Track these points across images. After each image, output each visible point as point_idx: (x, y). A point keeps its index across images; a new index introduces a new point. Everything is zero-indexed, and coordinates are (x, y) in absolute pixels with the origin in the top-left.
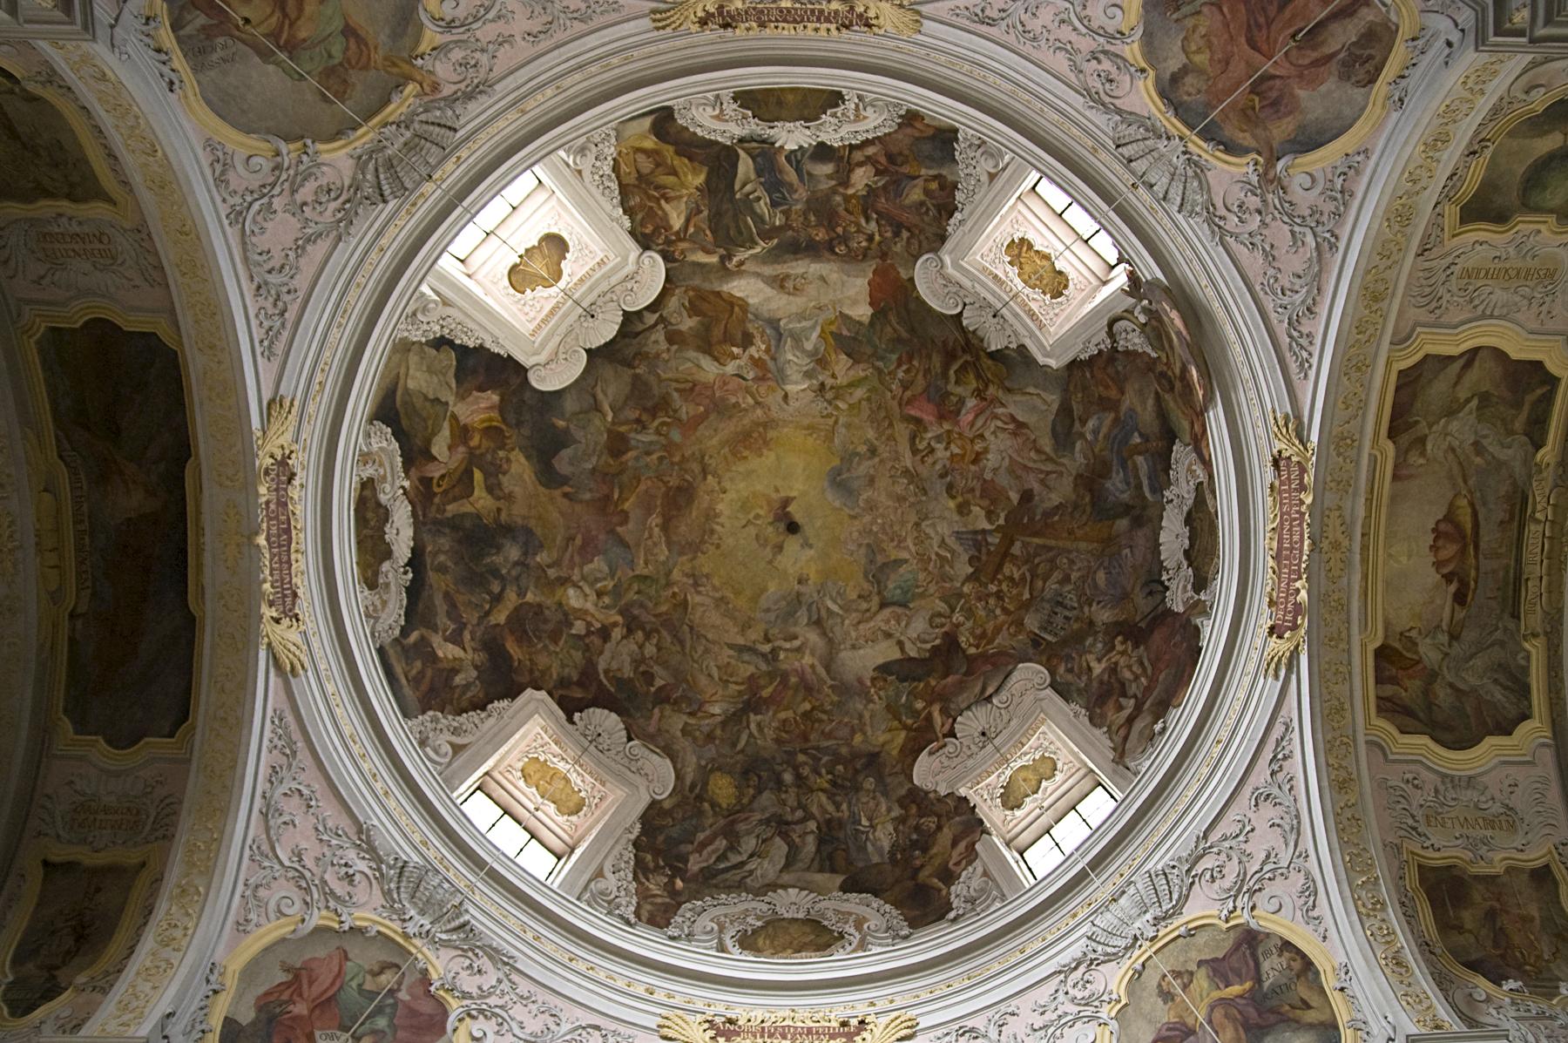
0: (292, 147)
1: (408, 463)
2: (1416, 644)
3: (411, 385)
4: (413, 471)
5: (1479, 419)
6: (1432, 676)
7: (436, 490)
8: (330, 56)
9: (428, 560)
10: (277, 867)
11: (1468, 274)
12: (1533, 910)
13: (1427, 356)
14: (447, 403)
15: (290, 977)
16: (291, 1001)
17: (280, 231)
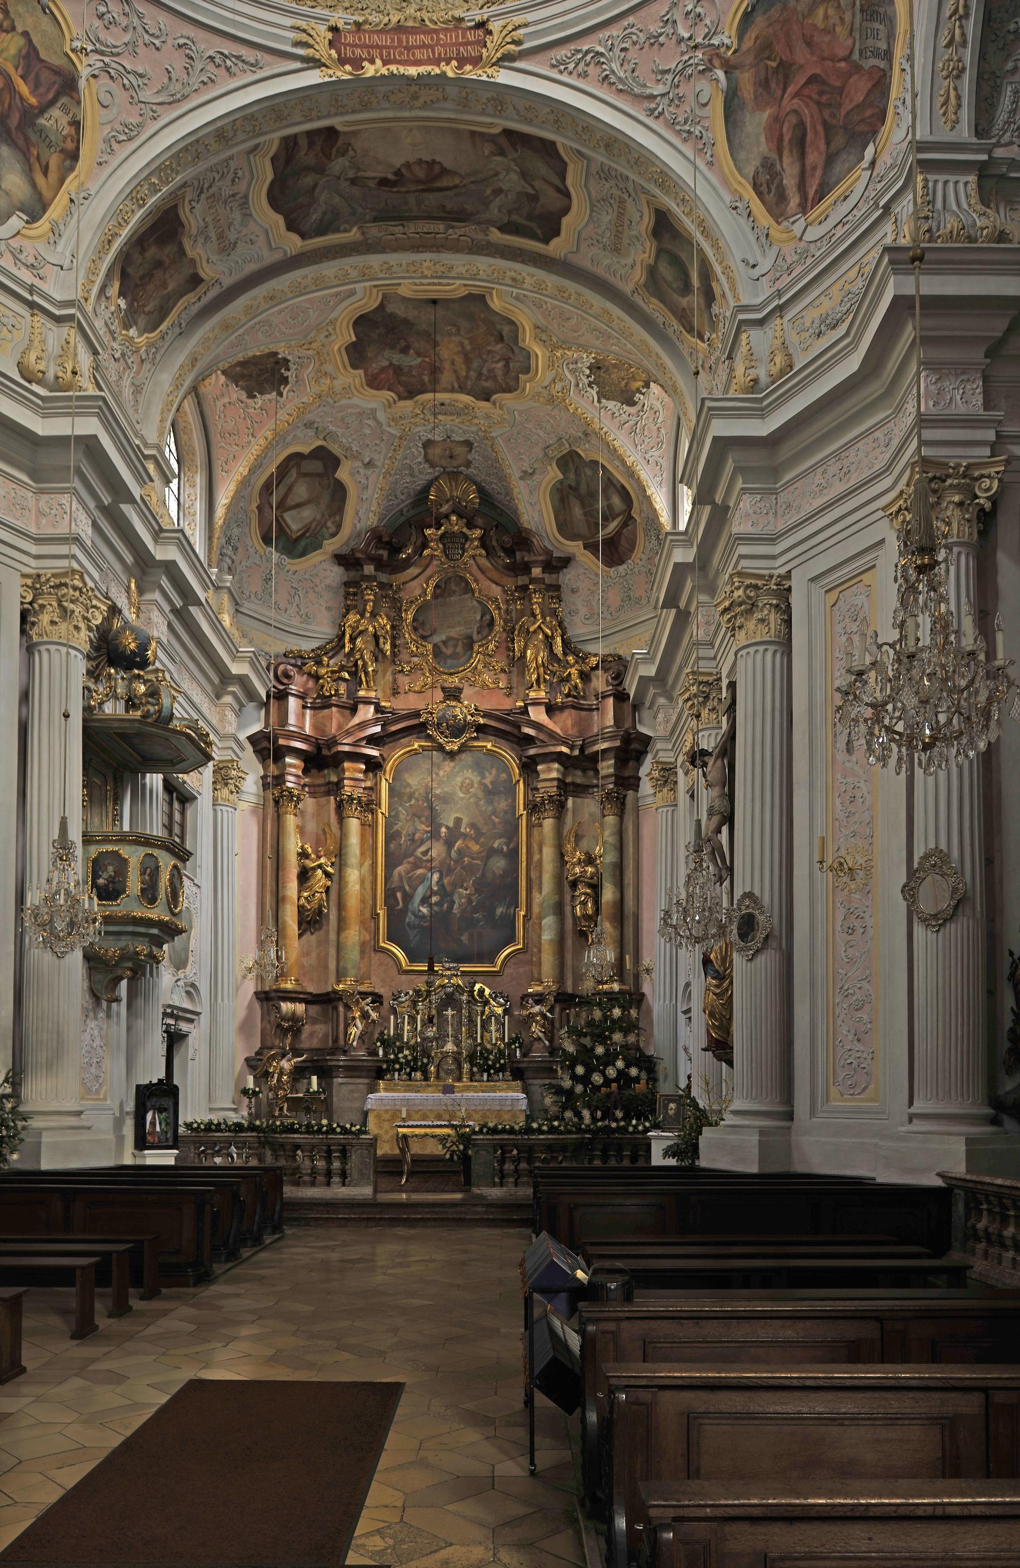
2: (343, 155)
5: (519, 194)
6: (320, 170)
11: (622, 202)
12: (172, 286)
13: (566, 164)
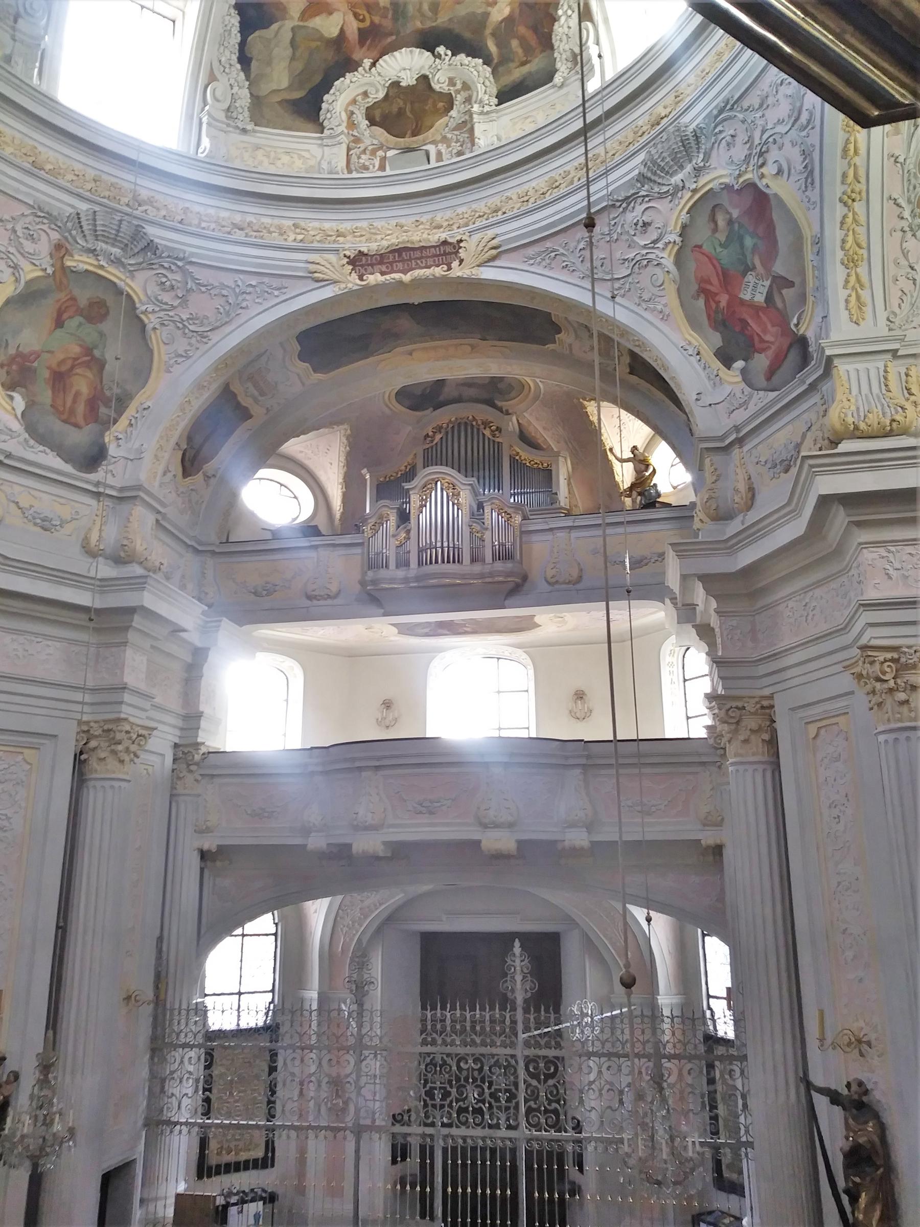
0: (146, 321)
1: (347, 65)
3: (285, 83)
4: (356, 56)
7: (367, 23)
8: (80, 324)
9: (429, 24)
10: (630, 280)
14: (293, 29)
15: (702, 295)
16: (717, 303)
17: (202, 305)
